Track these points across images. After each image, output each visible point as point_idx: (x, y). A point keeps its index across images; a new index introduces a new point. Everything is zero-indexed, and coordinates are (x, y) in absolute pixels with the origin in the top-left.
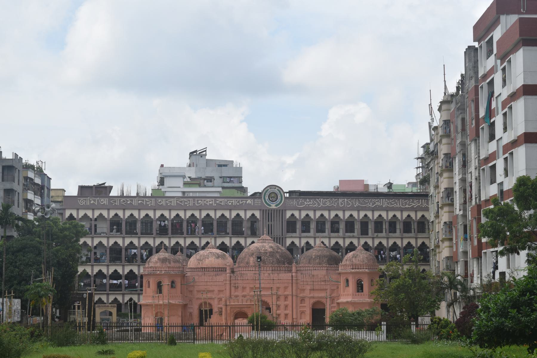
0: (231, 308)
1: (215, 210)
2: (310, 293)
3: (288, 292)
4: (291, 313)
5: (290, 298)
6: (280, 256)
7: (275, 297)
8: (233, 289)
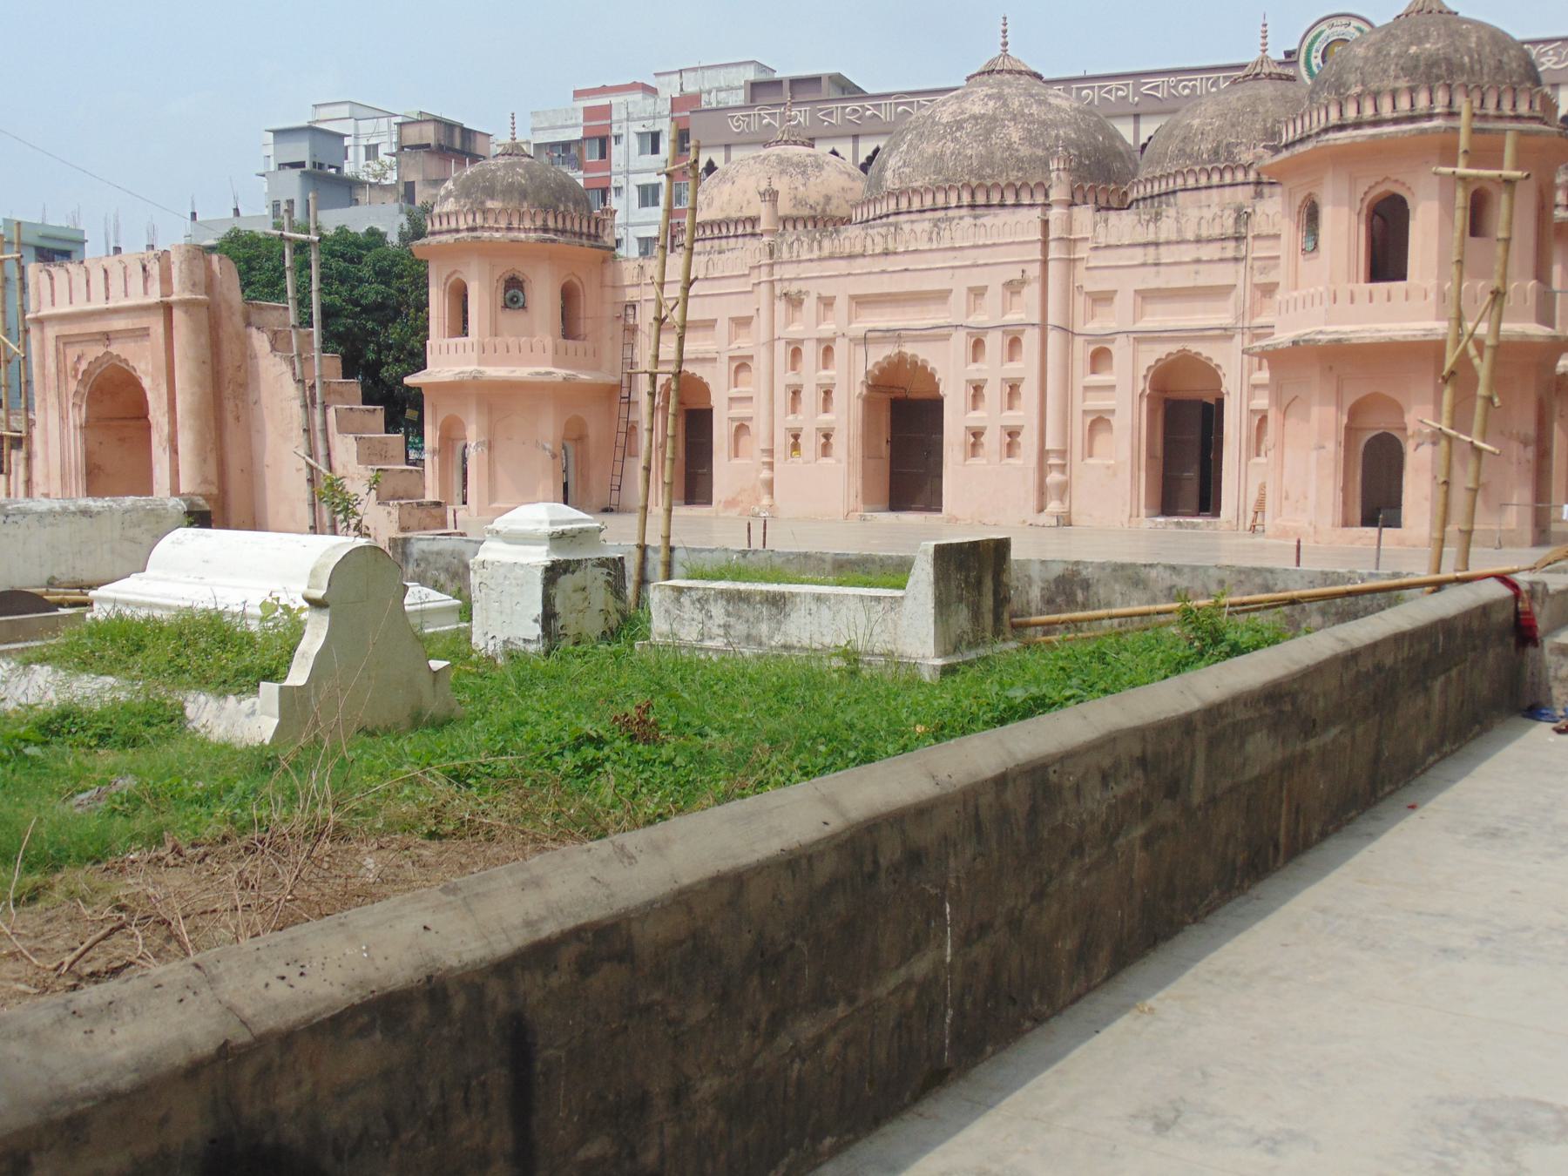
0: (64, 341)
1: (1137, 116)
2: (1138, 315)
3: (1024, 310)
4: (1035, 421)
5: (1030, 339)
6: (1029, 139)
7: (960, 341)
8: (781, 306)
